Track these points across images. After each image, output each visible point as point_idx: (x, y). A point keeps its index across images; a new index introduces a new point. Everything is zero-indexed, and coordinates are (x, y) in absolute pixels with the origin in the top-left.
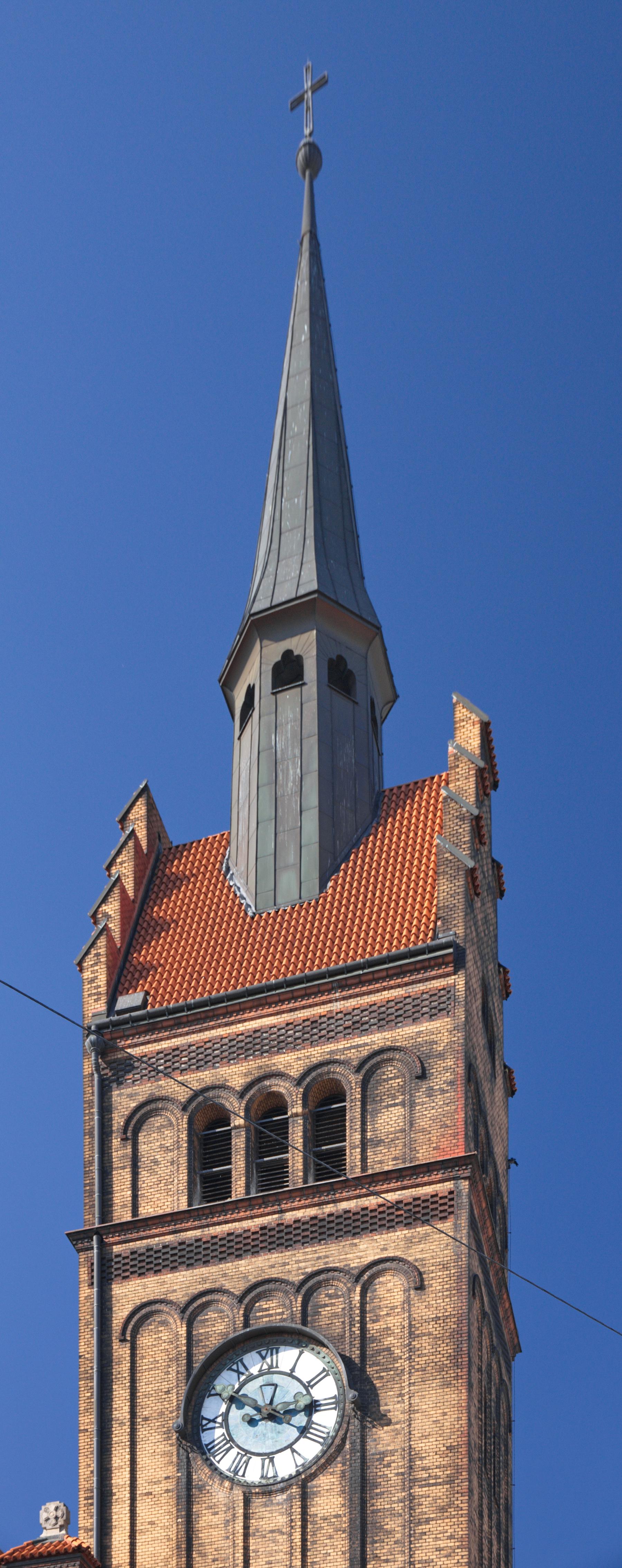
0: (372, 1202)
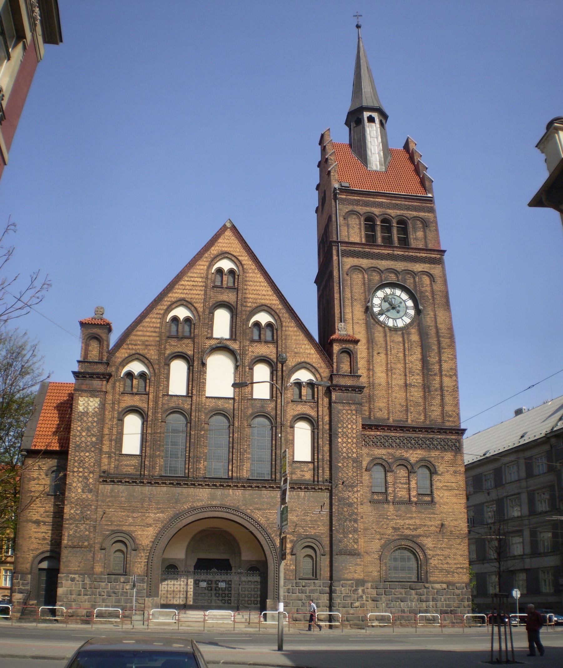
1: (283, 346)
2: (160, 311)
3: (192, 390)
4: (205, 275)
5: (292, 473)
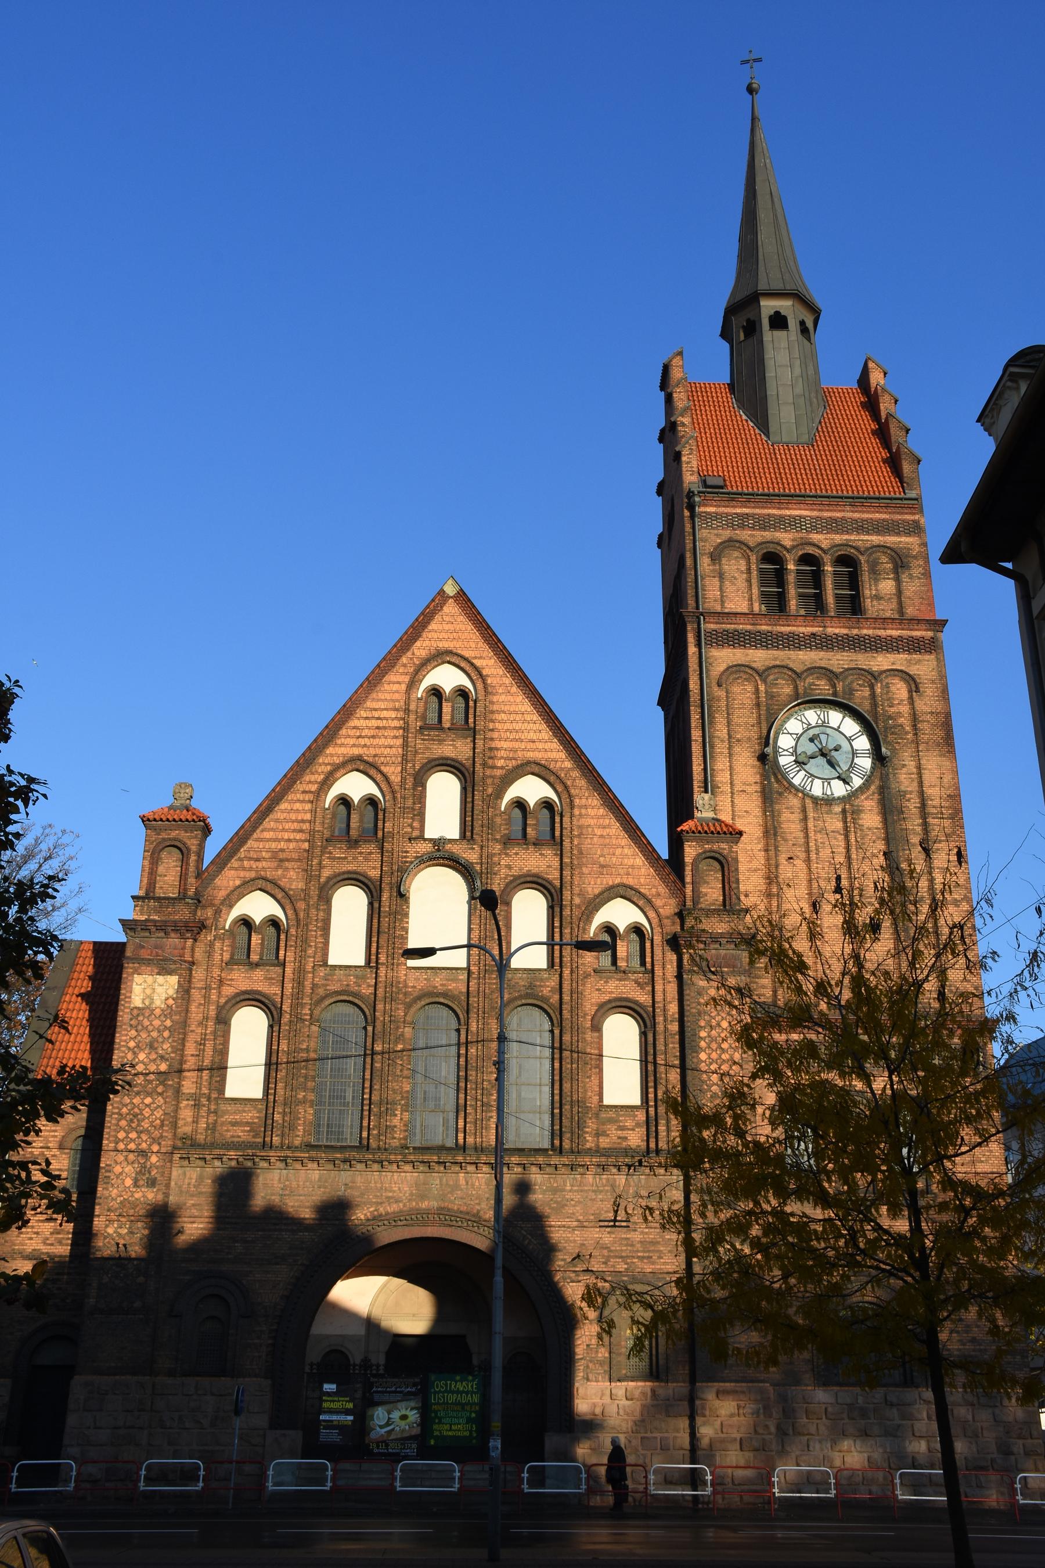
0: (882, 633)
1: (575, 852)
2: (310, 785)
3: (378, 953)
4: (402, 703)
5: (598, 1135)
